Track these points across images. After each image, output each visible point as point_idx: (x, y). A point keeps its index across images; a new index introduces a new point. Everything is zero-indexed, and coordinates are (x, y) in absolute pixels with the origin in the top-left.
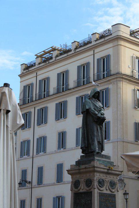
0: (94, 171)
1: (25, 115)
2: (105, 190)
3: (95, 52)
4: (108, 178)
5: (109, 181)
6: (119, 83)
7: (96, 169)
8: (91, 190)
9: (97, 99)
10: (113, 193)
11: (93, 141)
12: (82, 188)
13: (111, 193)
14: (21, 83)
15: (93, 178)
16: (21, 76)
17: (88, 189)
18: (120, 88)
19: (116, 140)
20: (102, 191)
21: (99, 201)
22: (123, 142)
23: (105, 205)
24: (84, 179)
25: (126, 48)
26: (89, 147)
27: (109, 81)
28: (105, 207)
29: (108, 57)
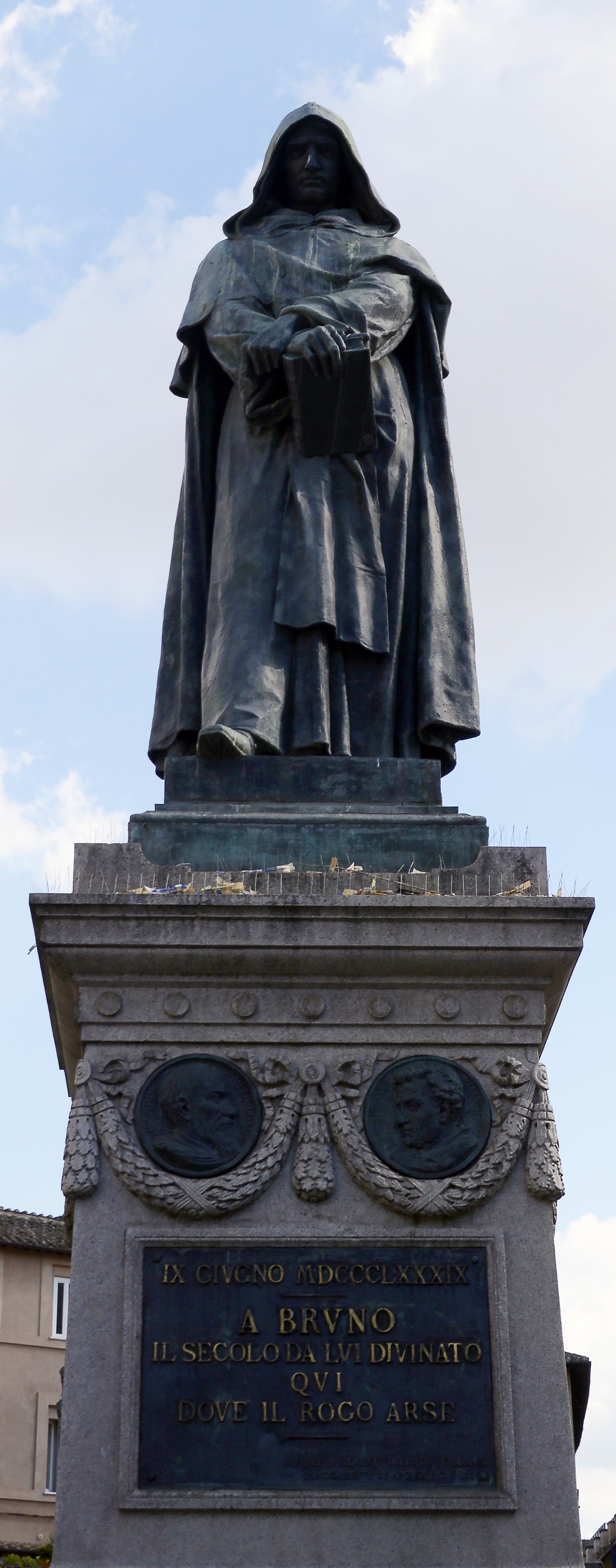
4: (330, 1035)
13: (403, 1232)
20: (221, 1215)
28: (266, 1440)
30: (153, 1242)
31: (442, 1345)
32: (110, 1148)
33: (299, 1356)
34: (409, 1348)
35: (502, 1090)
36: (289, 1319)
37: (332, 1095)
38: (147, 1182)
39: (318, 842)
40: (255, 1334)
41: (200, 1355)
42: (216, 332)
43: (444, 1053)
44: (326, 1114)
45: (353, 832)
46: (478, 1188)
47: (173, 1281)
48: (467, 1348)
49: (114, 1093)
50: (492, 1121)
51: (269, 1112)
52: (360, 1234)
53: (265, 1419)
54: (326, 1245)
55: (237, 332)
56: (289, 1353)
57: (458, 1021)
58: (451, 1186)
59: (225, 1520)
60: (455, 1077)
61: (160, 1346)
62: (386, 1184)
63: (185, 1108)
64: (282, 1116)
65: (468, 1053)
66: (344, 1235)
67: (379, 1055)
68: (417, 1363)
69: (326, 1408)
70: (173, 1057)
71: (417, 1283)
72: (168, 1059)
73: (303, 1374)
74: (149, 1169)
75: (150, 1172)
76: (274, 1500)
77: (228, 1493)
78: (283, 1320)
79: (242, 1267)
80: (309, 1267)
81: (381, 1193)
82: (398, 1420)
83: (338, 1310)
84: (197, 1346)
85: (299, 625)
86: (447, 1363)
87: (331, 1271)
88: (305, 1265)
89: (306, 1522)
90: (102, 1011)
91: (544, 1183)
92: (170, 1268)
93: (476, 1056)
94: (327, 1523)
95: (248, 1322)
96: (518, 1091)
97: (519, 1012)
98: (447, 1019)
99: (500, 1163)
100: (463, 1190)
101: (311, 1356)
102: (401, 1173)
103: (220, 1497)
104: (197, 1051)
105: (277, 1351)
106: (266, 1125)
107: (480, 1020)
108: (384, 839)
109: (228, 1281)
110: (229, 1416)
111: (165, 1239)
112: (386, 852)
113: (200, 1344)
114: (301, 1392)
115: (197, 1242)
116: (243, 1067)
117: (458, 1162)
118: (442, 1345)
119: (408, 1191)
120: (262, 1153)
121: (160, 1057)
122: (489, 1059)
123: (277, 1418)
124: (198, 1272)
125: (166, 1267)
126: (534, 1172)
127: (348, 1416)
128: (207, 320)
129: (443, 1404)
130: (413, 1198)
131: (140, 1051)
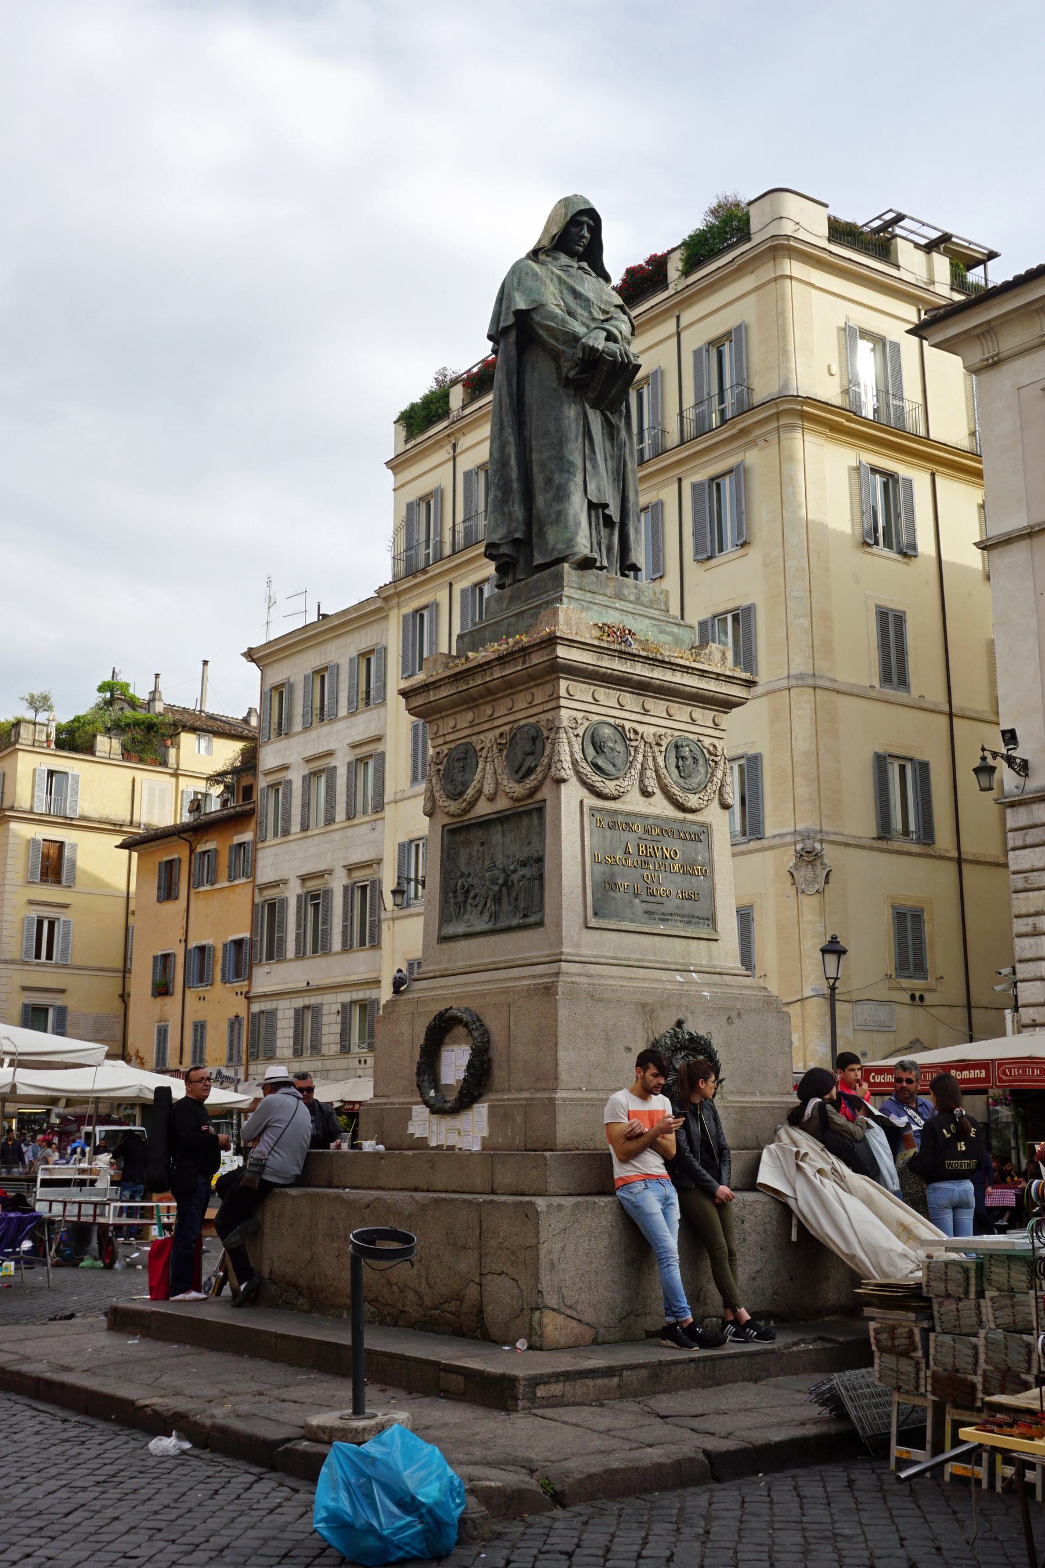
0: (556, 669)
1: (414, 617)
2: (635, 794)
3: (682, 324)
5: (664, 743)
6: (787, 435)
7: (562, 652)
8: (539, 796)
9: (585, 265)
10: (689, 817)
11: (561, 495)
12: (488, 788)
14: (398, 492)
15: (549, 716)
16: (396, 465)
17: (519, 789)
18: (791, 459)
19: (784, 683)
22: (814, 688)
23: (641, 888)
24: (497, 732)
25: (814, 291)
26: (535, 540)
27: (743, 432)
28: (637, 901)
29: (735, 336)
35: (713, 757)
43: (691, 736)
45: (648, 621)
51: (633, 753)
59: (623, 934)
65: (701, 738)
85: (595, 500)
89: (651, 937)
94: (657, 938)
106: (631, 759)
122: (707, 742)
126: (726, 796)
128: (533, 309)
131: (582, 714)
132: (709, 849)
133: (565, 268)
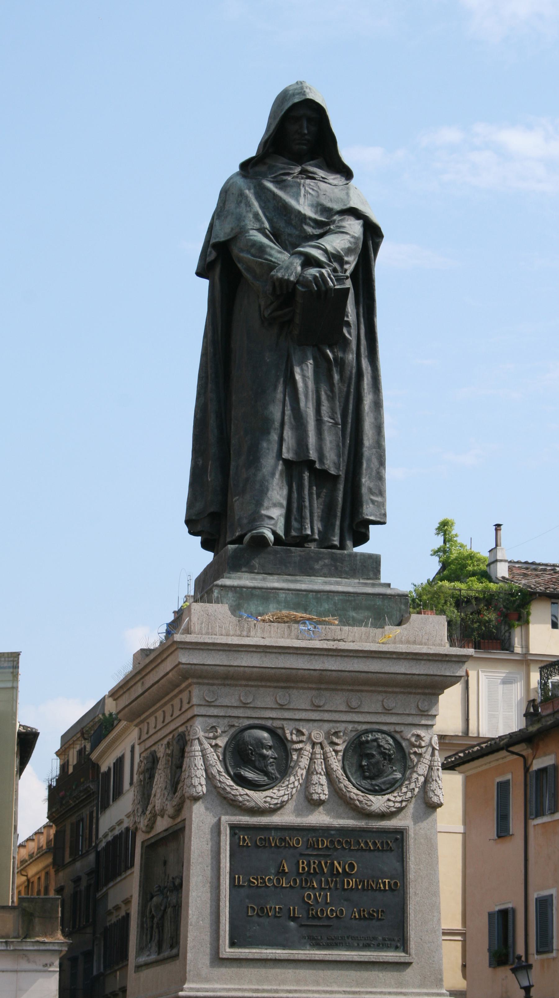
4: (326, 716)
21: (233, 885)
30: (235, 824)
31: (380, 881)
32: (212, 774)
33: (309, 884)
34: (364, 881)
36: (304, 865)
37: (328, 749)
38: (233, 793)
39: (317, 603)
40: (287, 873)
41: (259, 882)
42: (242, 250)
44: (324, 759)
46: (401, 802)
47: (245, 844)
48: (392, 882)
49: (213, 744)
50: (409, 766)
51: (295, 757)
52: (341, 823)
53: (292, 915)
54: (323, 828)
55: (260, 258)
56: (304, 883)
57: (393, 711)
58: (389, 800)
60: (391, 741)
61: (239, 878)
62: (355, 797)
63: (252, 753)
64: (302, 760)
66: (333, 823)
67: (352, 728)
68: (368, 890)
69: (322, 910)
70: (244, 725)
71: (368, 848)
72: (241, 725)
73: (311, 893)
74: (233, 786)
75: (234, 788)
76: (296, 955)
77: (274, 951)
78: (301, 866)
79: (281, 838)
80: (314, 839)
81: (352, 802)
82: (357, 917)
83: (329, 862)
84: (257, 878)
86: (382, 890)
87: (325, 842)
88: (312, 838)
90: (207, 699)
91: (435, 799)
92: (244, 838)
93: (401, 730)
95: (284, 867)
96: (424, 750)
97: (426, 708)
98: (389, 710)
99: (414, 789)
100: (394, 802)
101: (315, 884)
102: (363, 792)
103: (270, 953)
104: (257, 722)
105: (298, 881)
106: (292, 764)
107: (405, 711)
108: (353, 603)
109: (273, 845)
110: (273, 913)
111: (241, 823)
112: (354, 610)
113: (259, 877)
114: (310, 902)
115: (258, 825)
116: (280, 732)
117: (390, 787)
118: (380, 881)
119: (367, 802)
120: (292, 779)
121: (237, 725)
123: (298, 915)
124: (258, 840)
125: (242, 837)
126: (431, 794)
127: (333, 915)
129: (380, 910)
130: (369, 806)
132: (402, 858)
133: (279, 182)
